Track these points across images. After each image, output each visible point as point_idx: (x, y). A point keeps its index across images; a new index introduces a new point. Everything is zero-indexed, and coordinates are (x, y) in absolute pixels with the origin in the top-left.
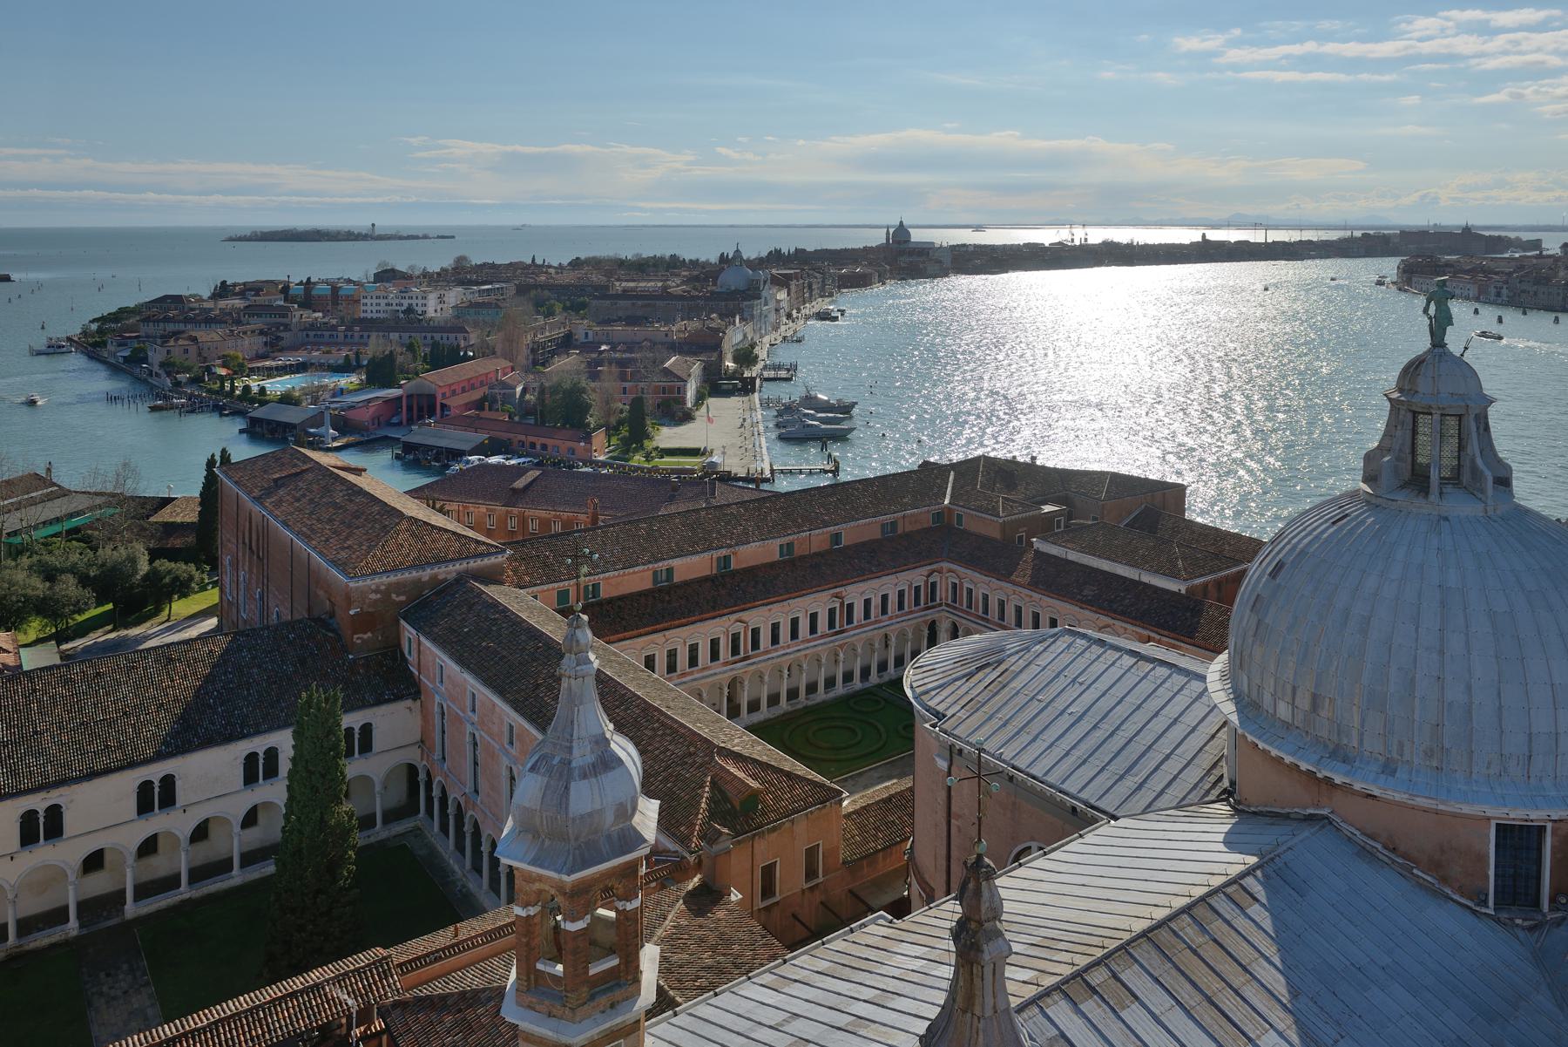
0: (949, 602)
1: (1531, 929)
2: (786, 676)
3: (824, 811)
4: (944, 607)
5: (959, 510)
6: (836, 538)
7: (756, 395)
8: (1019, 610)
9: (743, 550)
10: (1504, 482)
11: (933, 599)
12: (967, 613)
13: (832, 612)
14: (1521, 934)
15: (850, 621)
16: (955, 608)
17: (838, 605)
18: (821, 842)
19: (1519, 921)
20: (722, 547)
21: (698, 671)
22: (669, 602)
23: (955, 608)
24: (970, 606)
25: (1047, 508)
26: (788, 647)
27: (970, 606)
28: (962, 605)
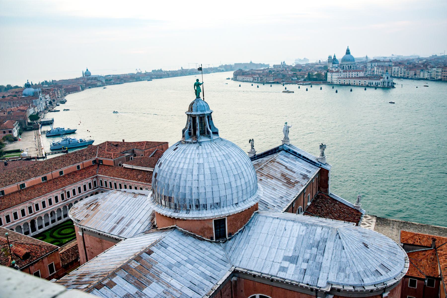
0: (100, 186)
1: (224, 243)
2: (50, 217)
3: (52, 254)
4: (99, 188)
5: (100, 158)
6: (61, 173)
7: (40, 130)
8: (120, 185)
9: (29, 181)
10: (216, 133)
11: (95, 186)
12: (106, 188)
13: (62, 195)
14: (221, 244)
15: (69, 196)
16: (102, 188)
17: (64, 193)
18: (53, 262)
19: (221, 241)
20: (21, 181)
21: (18, 220)
22: (4, 201)
23: (102, 188)
24: (106, 186)
25: (127, 154)
26: (49, 208)
27: (106, 186)
28: (104, 186)
